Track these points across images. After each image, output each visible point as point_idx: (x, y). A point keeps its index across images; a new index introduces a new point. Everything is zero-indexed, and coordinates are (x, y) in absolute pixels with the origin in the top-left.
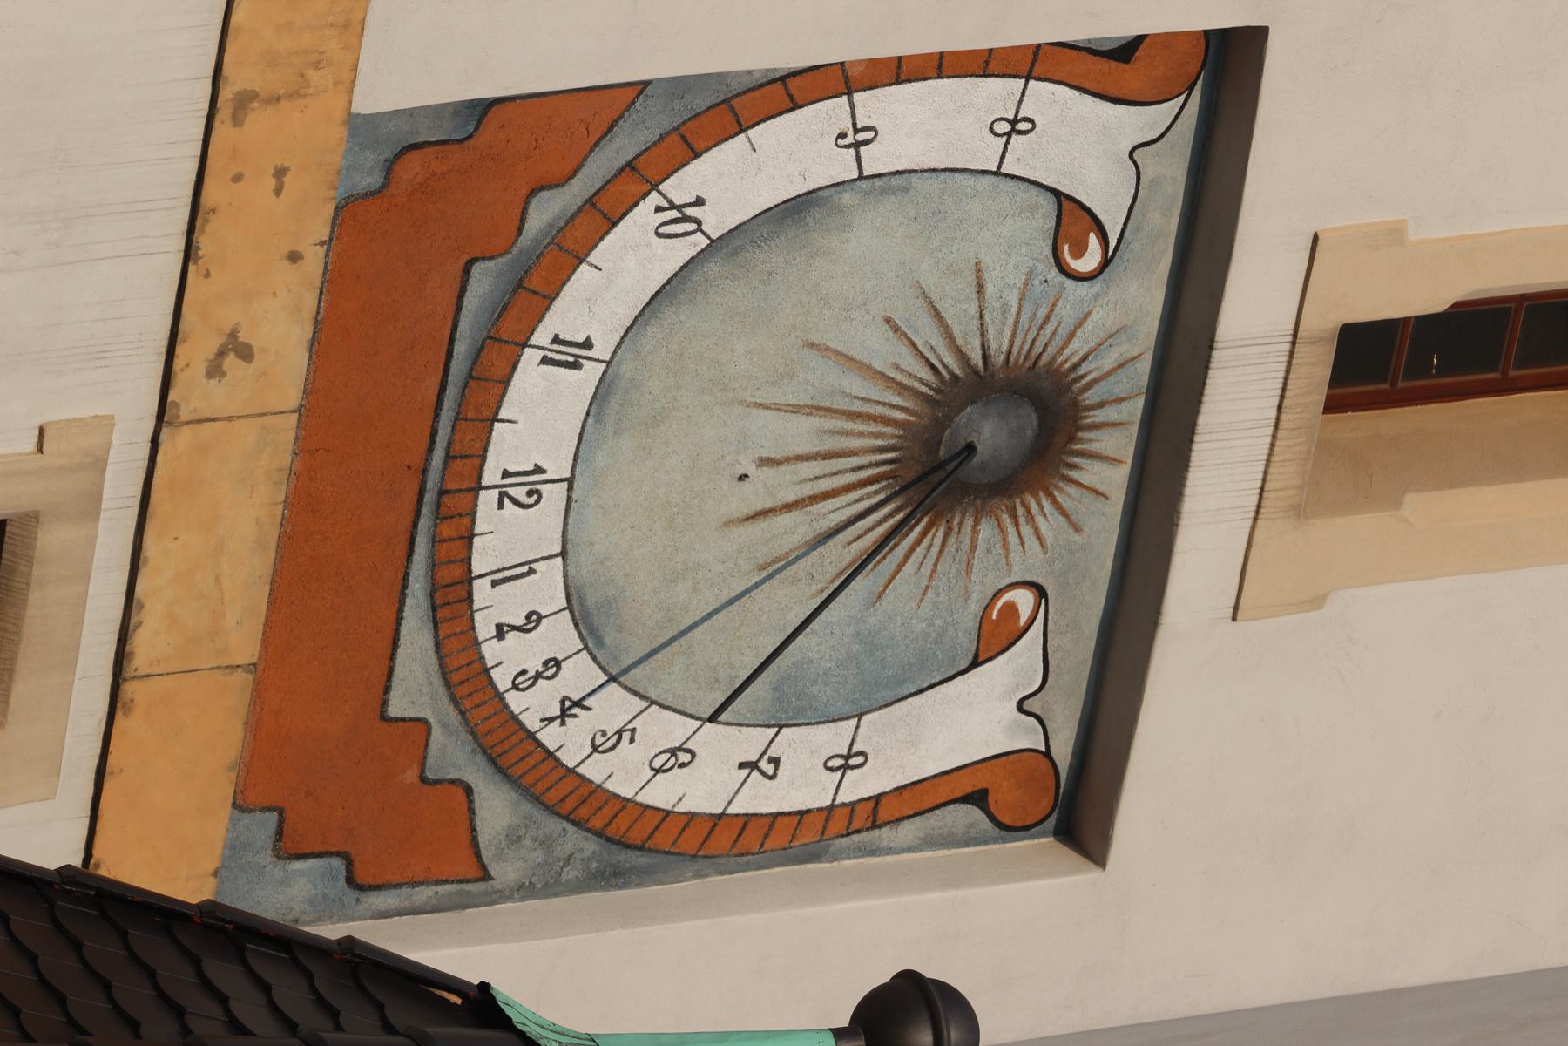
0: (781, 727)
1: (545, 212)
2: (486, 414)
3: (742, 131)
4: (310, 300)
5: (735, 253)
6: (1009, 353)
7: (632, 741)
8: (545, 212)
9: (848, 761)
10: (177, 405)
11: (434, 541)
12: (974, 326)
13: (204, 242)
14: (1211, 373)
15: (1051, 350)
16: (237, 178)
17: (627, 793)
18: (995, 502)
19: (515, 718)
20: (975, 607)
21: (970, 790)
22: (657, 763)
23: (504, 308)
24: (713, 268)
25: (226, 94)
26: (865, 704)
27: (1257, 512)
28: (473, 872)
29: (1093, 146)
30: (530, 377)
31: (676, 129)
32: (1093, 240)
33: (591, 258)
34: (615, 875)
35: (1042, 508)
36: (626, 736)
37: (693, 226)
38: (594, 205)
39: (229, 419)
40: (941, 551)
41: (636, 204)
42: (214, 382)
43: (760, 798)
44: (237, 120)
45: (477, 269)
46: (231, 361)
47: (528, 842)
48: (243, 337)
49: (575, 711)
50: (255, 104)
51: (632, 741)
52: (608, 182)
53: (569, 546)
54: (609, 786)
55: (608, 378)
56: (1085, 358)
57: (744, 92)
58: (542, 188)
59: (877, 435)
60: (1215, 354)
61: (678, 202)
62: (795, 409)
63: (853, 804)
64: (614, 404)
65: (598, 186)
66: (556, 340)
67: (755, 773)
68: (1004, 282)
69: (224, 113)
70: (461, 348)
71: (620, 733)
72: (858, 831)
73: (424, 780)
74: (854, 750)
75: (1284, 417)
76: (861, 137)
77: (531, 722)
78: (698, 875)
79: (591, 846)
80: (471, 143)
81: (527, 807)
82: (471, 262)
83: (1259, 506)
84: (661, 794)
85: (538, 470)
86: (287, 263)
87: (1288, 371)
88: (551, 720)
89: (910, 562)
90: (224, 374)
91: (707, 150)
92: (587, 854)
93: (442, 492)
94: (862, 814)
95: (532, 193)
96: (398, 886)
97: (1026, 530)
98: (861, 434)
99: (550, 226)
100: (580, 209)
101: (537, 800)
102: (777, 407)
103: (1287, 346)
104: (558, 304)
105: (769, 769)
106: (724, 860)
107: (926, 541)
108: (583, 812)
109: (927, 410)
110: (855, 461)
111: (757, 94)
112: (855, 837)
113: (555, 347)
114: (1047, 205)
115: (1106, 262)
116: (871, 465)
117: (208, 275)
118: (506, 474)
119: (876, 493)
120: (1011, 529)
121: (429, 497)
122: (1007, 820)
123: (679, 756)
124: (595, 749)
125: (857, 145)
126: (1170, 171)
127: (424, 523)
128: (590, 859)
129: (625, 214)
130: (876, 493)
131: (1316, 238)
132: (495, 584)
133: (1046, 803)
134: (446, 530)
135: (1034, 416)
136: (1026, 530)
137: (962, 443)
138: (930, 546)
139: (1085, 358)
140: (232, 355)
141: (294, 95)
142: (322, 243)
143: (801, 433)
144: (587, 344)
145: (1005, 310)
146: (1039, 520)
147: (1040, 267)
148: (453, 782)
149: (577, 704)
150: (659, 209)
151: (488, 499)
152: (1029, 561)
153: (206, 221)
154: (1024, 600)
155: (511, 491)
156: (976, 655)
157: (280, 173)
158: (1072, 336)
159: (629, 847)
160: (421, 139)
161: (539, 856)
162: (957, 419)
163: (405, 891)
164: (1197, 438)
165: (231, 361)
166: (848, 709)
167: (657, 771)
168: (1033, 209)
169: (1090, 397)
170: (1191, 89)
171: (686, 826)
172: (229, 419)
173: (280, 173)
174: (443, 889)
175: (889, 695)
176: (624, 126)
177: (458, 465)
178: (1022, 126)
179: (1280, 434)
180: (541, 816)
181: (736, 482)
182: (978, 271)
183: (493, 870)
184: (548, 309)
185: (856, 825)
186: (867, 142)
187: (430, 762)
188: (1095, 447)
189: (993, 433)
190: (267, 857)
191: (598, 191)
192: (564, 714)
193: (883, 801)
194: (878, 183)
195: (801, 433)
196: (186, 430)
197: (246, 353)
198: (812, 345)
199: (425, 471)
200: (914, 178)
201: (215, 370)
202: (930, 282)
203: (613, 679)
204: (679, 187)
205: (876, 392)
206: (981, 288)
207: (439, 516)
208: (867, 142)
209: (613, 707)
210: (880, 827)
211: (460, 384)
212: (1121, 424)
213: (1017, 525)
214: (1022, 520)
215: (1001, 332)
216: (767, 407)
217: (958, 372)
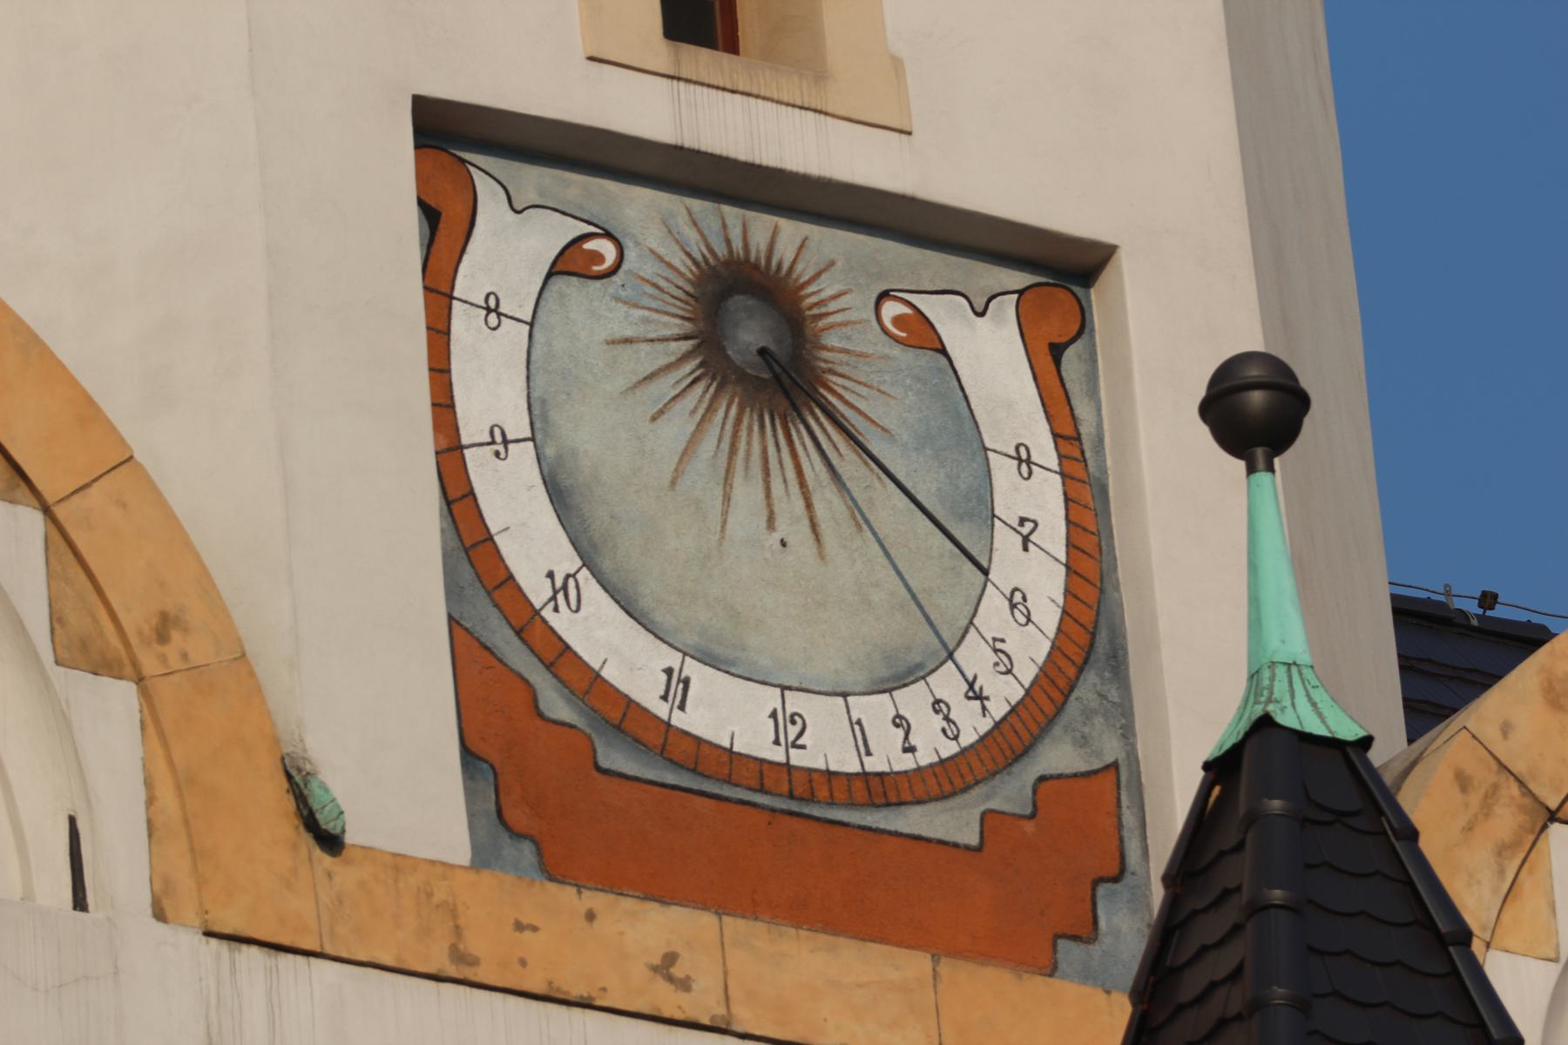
0: (994, 516)
1: (557, 705)
2: (725, 758)
3: (490, 538)
4: (628, 904)
5: (594, 546)
6: (683, 318)
7: (1003, 641)
8: (557, 705)
9: (1023, 459)
10: (713, 1018)
11: (832, 803)
12: (659, 346)
13: (577, 991)
14: (703, 148)
15: (681, 283)
16: (523, 963)
17: (1046, 647)
18: (808, 332)
19: (982, 739)
20: (896, 351)
21: (1049, 358)
22: (1023, 620)
23: (637, 741)
24: (606, 565)
25: (452, 971)
26: (975, 445)
27: (820, 112)
28: (1111, 775)
29: (510, 244)
30: (695, 720)
31: (489, 593)
32: (589, 245)
33: (596, 666)
34: (1115, 657)
35: (814, 293)
36: (999, 645)
37: (571, 581)
38: (552, 664)
39: (726, 973)
40: (848, 378)
41: (551, 629)
42: (694, 986)
43: (1053, 534)
44: (474, 962)
45: (604, 763)
46: (678, 971)
47: (1086, 730)
48: (657, 961)
49: (977, 688)
50: (461, 947)
51: (1003, 641)
52: (532, 651)
53: (839, 690)
54: (1041, 660)
55: (698, 655)
56: (688, 255)
57: (459, 536)
58: (537, 707)
59: (750, 429)
60: (687, 145)
61: (550, 593)
62: (727, 498)
63: (1060, 457)
64: (719, 650)
65: (535, 660)
66: (665, 698)
67: (1032, 538)
68: (622, 321)
69: (468, 973)
70: (670, 778)
71: (996, 651)
72: (1083, 453)
73: (1033, 816)
74: (1013, 453)
75: (741, 88)
76: (498, 438)
77: (985, 725)
78: (1117, 588)
79: (1090, 678)
80: (497, 766)
81: (1057, 730)
83: (815, 111)
84: (1048, 617)
85: (774, 715)
86: (596, 923)
87: (702, 84)
88: (984, 708)
89: (858, 404)
90: (688, 978)
91: (507, 568)
92: (1097, 680)
93: (791, 796)
94: (1068, 449)
95: (541, 715)
96: (1121, 840)
97: (832, 306)
98: (749, 444)
99: (568, 701)
100: (555, 676)
101: (1051, 721)
102: (725, 513)
103: (682, 84)
104: (635, 695)
105: (1029, 526)
106: (1105, 566)
107: (840, 390)
108: (1062, 683)
109: (730, 388)
110: (771, 449)
111: (461, 526)
112: (1088, 455)
113: (670, 698)
114: (559, 283)
115: (608, 235)
116: (775, 436)
117: (604, 989)
118: (777, 742)
119: (798, 431)
120: (831, 319)
121: (794, 806)
122: (1076, 327)
123: (1016, 601)
124: (1009, 672)
125: (506, 442)
126: (532, 179)
127: (817, 811)
128: (1102, 678)
129: (560, 638)
130: (798, 431)
131: (591, 59)
132: (869, 753)
133: (1062, 295)
134: (823, 793)
135: (737, 298)
136: (832, 306)
137: (758, 359)
138: (844, 388)
139: (688, 255)
140: (672, 970)
141: (454, 914)
142: (579, 892)
143: (747, 492)
145: (646, 321)
146: (823, 295)
147: (611, 290)
148: (1035, 792)
149: (971, 685)
150: (556, 609)
151: (798, 759)
152: (858, 305)
153: (558, 990)
154: (891, 310)
155: (791, 738)
156: (937, 350)
157: (520, 927)
158: (669, 265)
159: (1092, 645)
160: (493, 807)
161: (1098, 720)
162: (738, 362)
163: (1125, 833)
164: (757, 161)
166: (980, 459)
167: (1029, 620)
169: (721, 251)
170: (463, 161)
171: (1075, 596)
172: (726, 973)
173: (520, 927)
174: (1125, 801)
175: (968, 424)
177: (768, 783)
178: (492, 303)
179: (755, 91)
180: (1064, 719)
181: (788, 549)
182: (613, 342)
183: (1109, 759)
184: (638, 705)
185: (1077, 454)
186: (503, 434)
187: (1018, 811)
188: (763, 247)
189: (750, 333)
190: (1096, 949)
191: (540, 660)
192: (980, 697)
193: (1058, 431)
194: (538, 425)
195: (747, 492)
196: (735, 1009)
197: (671, 958)
198: (673, 483)
199: (773, 810)
200: (535, 395)
201: (685, 985)
202: (621, 383)
203: (950, 656)
204: (537, 591)
205: (713, 431)
206: (628, 341)
207: (811, 798)
208: (503, 434)
209: (976, 656)
210: (1079, 434)
211: (700, 779)
212: (744, 225)
213: (828, 314)
214: (824, 310)
215: (665, 325)
216: (724, 522)
217: (697, 361)
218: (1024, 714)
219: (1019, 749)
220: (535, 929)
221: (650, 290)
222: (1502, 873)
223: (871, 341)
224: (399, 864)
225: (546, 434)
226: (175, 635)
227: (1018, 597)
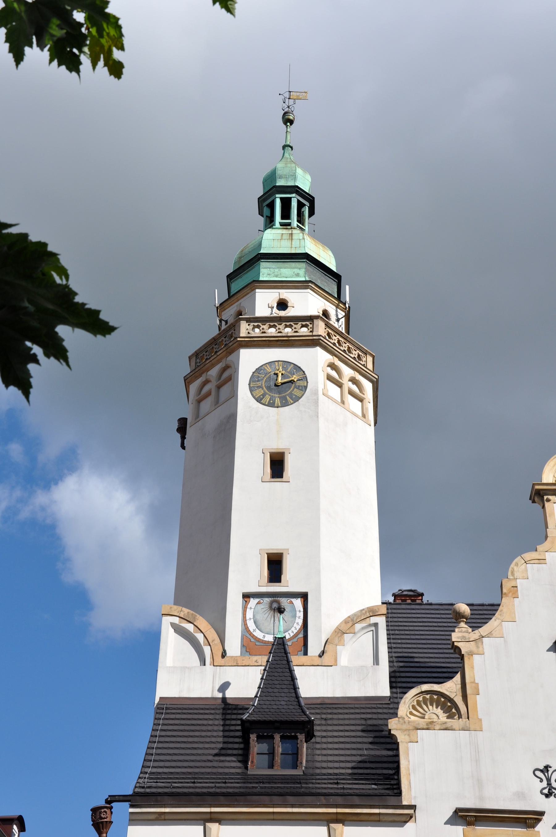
1: (252, 640)
8: (252, 640)
9: (300, 611)
30: (266, 639)
43: (302, 617)
68: (263, 607)
123: (298, 623)
189: (275, 605)
204: (252, 631)
223: (287, 604)
224: (232, 657)
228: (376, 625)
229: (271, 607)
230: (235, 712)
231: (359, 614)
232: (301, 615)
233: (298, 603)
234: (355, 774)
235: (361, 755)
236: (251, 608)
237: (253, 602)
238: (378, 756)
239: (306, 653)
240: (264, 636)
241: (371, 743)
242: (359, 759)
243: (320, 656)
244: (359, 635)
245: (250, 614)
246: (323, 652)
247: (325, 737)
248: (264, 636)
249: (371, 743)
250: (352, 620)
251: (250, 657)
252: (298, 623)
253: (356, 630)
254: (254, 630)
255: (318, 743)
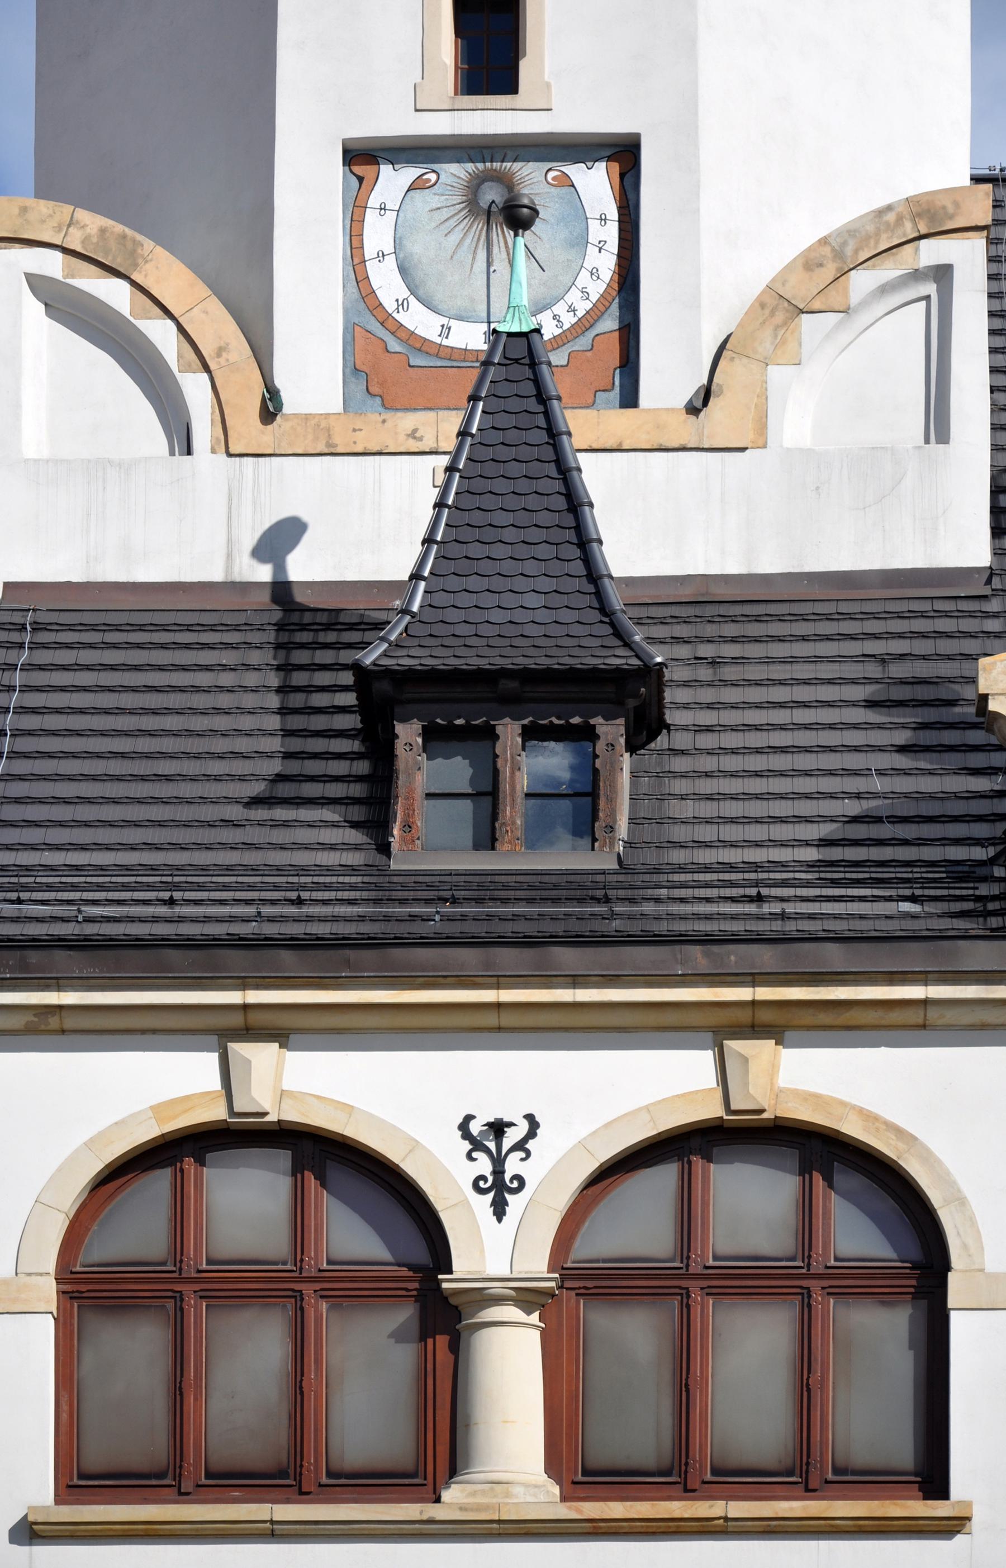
1: (394, 345)
8: (394, 345)
9: (603, 219)
12: (452, 208)
13: (375, 450)
16: (355, 443)
19: (572, 326)
20: (553, 189)
22: (595, 278)
24: (421, 292)
26: (583, 218)
44: (336, 446)
46: (417, 435)
62: (474, 258)
64: (464, 314)
70: (439, 364)
77: (575, 320)
81: (606, 316)
82: (410, 366)
95: (388, 351)
101: (603, 314)
123: (594, 273)
125: (383, 256)
141: (329, 430)
144: (443, 326)
154: (551, 175)
157: (354, 430)
158: (459, 177)
165: (417, 435)
166: (584, 223)
168: (412, 198)
173: (354, 430)
174: (631, 337)
176: (369, 328)
180: (609, 312)
189: (492, 195)
197: (415, 430)
201: (421, 439)
202: (434, 224)
204: (390, 306)
218: (592, 313)
219: (588, 325)
220: (361, 430)
221: (450, 188)
222: (776, 336)
224: (307, 417)
225: (400, 249)
226: (224, 355)
227: (595, 270)
228: (942, 274)
229: (472, 205)
230: (331, 637)
231: (870, 228)
232: (611, 234)
233: (595, 183)
234: (832, 863)
235: (858, 796)
236: (383, 208)
237: (392, 181)
238: (931, 797)
239: (630, 399)
240: (446, 331)
241: (902, 749)
242: (853, 808)
243: (693, 410)
244: (865, 318)
245: (378, 233)
246: (707, 394)
247: (709, 729)
248: (446, 331)
249: (902, 749)
250: (838, 255)
251: (387, 415)
252: (594, 273)
253: (854, 299)
254: (402, 305)
255: (683, 752)
